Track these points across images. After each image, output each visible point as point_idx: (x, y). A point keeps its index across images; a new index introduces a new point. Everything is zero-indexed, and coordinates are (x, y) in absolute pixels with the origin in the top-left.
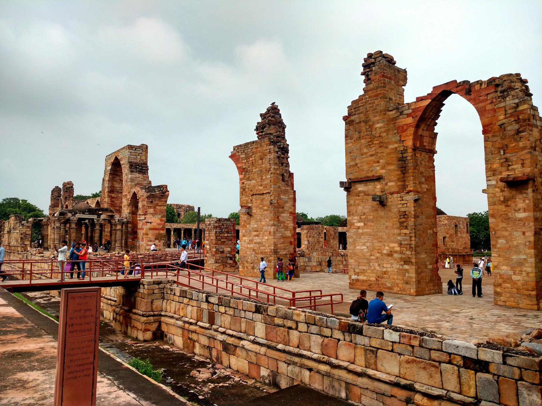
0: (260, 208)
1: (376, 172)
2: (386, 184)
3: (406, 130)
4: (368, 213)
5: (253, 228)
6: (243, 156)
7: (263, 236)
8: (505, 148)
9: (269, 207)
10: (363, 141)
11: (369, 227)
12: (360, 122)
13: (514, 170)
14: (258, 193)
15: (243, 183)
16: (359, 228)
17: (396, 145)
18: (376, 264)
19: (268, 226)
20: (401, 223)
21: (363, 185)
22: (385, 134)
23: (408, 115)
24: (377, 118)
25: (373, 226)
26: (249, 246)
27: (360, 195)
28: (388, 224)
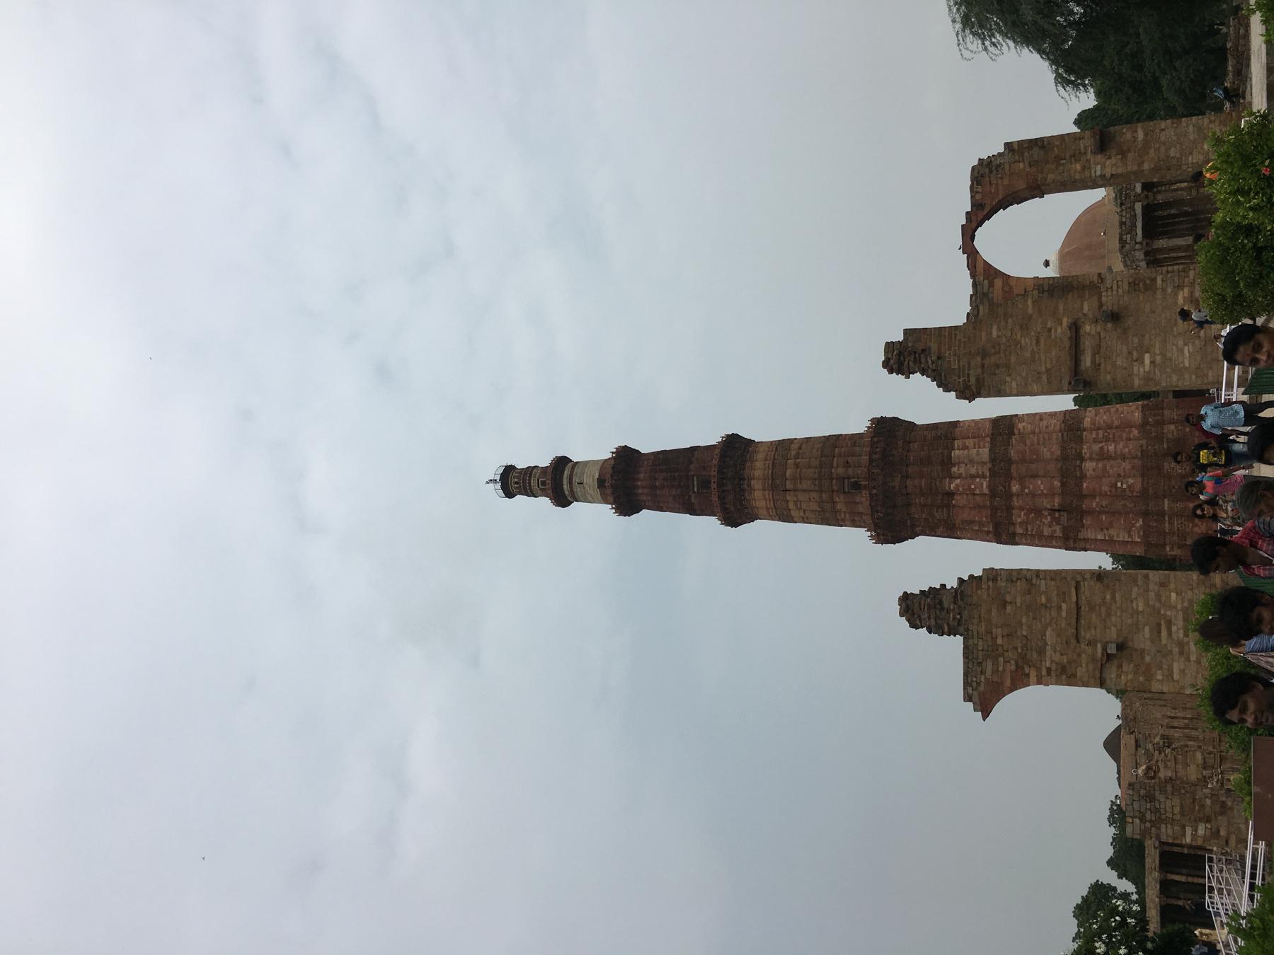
0: (1109, 615)
2: (1085, 315)
3: (1011, 288)
5: (1152, 641)
8: (1058, 159)
10: (1013, 359)
12: (983, 366)
13: (1085, 147)
14: (1074, 621)
15: (1049, 670)
16: (1153, 362)
19: (1147, 591)
20: (1146, 289)
23: (991, 285)
24: (984, 334)
26: (1193, 658)
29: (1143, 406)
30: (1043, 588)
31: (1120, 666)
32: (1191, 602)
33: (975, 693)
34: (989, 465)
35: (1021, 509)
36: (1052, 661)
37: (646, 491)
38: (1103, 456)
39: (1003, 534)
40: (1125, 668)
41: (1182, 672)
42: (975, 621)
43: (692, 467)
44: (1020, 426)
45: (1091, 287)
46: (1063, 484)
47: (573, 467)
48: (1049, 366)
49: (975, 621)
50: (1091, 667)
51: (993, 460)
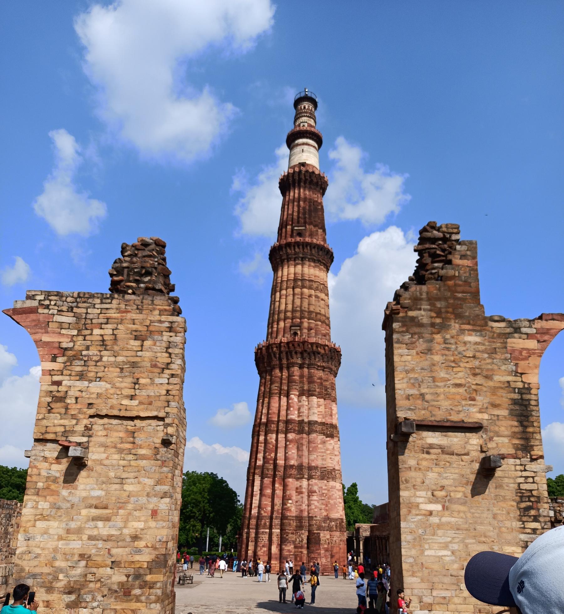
0: (121, 451)
4: (451, 486)
5: (85, 499)
11: (455, 514)
14: (115, 412)
16: (431, 513)
21: (437, 434)
25: (464, 512)
27: (432, 451)
29: (342, 519)
30: (158, 381)
34: (306, 420)
35: (277, 440)
37: (296, 195)
38: (311, 493)
39: (259, 428)
44: (332, 442)
45: (526, 445)
46: (292, 467)
48: (428, 397)
51: (310, 423)
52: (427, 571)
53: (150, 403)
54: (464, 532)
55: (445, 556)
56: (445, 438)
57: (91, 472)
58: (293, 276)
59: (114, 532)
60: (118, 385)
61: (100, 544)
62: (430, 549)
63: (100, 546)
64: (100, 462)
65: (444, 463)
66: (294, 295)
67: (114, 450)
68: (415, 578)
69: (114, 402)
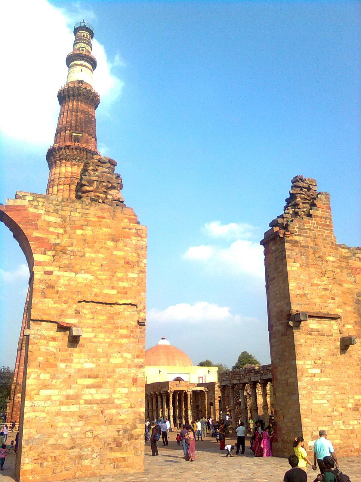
0: (106, 331)
1: (332, 309)
2: (344, 326)
5: (79, 370)
6: (51, 219)
7: (113, 386)
9: (132, 332)
10: (313, 270)
11: (328, 375)
14: (99, 300)
15: (50, 273)
16: (314, 375)
17: (351, 286)
18: (341, 422)
19: (129, 367)
21: (315, 322)
22: (339, 270)
26: (64, 409)
27: (313, 333)
28: (349, 372)
30: (131, 275)
31: (54, 339)
32: (118, 407)
33: (26, 203)
36: (59, 277)
40: (52, 344)
41: (48, 398)
42: (99, 213)
43: (87, 135)
47: (90, 69)
48: (309, 296)
49: (99, 213)
50: (53, 312)
52: (315, 414)
53: (126, 293)
54: (333, 387)
55: (324, 403)
56: (320, 325)
57: (82, 348)
58: (69, 174)
59: (105, 397)
60: (99, 277)
61: (95, 407)
62: (315, 399)
63: (95, 408)
64: (90, 340)
65: (320, 341)
66: (70, 190)
67: (99, 330)
68: (308, 419)
69: (96, 290)
